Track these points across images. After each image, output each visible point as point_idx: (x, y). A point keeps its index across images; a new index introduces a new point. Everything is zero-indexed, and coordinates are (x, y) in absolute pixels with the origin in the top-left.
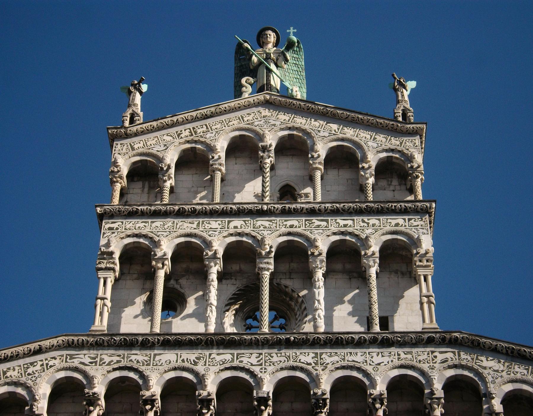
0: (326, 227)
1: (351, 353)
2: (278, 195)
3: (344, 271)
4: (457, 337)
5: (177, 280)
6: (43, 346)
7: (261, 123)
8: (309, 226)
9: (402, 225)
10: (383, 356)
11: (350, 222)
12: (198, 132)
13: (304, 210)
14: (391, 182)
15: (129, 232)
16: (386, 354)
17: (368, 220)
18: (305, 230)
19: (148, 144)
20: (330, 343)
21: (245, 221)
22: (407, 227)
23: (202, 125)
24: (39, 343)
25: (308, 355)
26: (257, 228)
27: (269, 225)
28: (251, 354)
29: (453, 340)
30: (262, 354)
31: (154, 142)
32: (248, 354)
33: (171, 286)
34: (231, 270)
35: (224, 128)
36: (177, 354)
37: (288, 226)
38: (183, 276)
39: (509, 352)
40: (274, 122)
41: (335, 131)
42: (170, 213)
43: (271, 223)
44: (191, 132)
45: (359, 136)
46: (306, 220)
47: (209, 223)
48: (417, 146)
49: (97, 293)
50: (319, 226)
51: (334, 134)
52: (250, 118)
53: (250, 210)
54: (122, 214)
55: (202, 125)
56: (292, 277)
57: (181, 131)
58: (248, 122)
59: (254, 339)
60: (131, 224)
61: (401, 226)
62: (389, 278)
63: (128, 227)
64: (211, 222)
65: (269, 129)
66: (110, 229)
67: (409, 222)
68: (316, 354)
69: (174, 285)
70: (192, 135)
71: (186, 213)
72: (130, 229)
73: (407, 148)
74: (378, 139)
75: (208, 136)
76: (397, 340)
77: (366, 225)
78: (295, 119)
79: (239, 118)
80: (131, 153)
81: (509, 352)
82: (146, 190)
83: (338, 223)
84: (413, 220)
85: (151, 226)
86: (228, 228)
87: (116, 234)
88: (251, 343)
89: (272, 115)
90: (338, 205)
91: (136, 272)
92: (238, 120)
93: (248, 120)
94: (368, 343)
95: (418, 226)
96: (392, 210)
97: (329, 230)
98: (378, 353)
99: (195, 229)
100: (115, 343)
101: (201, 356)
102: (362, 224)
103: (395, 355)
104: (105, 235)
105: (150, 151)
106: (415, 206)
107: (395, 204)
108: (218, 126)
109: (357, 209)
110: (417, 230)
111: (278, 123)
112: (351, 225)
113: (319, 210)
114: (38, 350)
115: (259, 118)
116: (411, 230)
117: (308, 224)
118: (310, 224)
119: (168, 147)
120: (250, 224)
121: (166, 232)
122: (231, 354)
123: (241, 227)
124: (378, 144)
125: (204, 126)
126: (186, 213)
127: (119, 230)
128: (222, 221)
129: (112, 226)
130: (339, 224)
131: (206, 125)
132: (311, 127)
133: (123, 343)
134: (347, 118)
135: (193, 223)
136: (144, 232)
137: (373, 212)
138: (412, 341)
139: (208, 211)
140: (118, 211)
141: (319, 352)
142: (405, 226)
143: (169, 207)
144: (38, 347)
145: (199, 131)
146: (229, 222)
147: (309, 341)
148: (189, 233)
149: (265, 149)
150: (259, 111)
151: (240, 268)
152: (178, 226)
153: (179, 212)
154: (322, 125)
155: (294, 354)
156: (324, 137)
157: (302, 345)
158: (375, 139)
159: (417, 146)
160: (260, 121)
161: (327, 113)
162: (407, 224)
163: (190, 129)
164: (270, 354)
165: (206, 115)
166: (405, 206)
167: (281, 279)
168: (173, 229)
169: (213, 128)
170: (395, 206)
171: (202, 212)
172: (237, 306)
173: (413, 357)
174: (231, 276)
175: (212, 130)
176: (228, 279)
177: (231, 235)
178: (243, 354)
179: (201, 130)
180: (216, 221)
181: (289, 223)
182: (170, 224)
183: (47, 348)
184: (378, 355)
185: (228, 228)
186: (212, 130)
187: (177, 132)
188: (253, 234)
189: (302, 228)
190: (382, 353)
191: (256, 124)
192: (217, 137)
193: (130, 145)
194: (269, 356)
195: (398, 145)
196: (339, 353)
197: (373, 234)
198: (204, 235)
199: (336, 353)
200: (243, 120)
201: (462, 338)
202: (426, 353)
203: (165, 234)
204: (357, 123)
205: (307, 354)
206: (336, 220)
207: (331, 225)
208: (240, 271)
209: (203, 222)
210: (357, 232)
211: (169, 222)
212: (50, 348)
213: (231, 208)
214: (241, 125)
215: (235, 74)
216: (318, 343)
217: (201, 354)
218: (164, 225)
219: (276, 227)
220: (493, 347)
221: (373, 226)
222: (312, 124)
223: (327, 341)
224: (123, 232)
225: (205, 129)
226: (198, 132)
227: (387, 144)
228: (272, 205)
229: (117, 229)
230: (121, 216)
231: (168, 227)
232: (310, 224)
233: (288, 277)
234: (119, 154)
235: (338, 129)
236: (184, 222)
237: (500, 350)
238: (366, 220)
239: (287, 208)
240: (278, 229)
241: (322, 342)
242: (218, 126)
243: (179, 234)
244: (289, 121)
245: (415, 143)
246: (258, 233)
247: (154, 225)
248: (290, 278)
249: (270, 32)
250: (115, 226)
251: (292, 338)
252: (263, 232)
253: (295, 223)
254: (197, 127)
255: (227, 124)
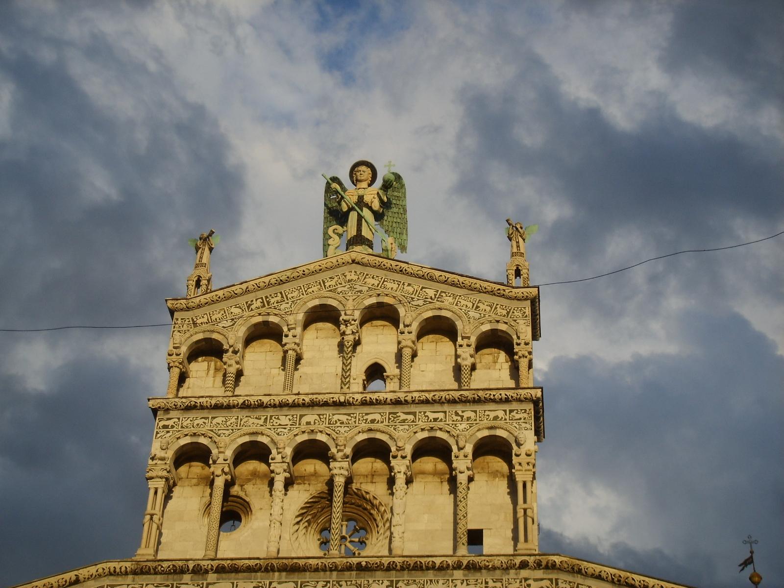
0: (413, 421)
1: (431, 581)
2: (364, 378)
3: (435, 473)
4: (555, 562)
5: (242, 486)
6: (81, 578)
7: (345, 289)
8: (394, 420)
9: (502, 418)
10: (468, 585)
11: (441, 416)
12: (272, 302)
13: (388, 400)
14: (498, 359)
15: (186, 431)
16: (472, 582)
17: (463, 412)
18: (388, 426)
19: (213, 318)
20: (408, 568)
21: (319, 415)
22: (508, 421)
23: (276, 294)
24: (76, 573)
25: (382, 584)
26: (333, 424)
27: (347, 419)
28: (317, 582)
29: (550, 565)
30: (329, 582)
31: (220, 316)
32: (313, 583)
33: (235, 493)
34: (304, 472)
35: (302, 296)
36: (233, 583)
37: (368, 420)
38: (249, 480)
39: (616, 579)
40: (359, 288)
41: (431, 298)
42: (234, 407)
43: (350, 418)
44: (263, 302)
45: (459, 305)
46: (390, 413)
47: (278, 419)
48: (526, 316)
49: (146, 509)
50: (404, 421)
51: (430, 303)
52: (333, 283)
53: (325, 401)
54: (179, 408)
55: (276, 294)
56: (374, 481)
57: (252, 301)
58: (330, 289)
59: (320, 564)
60: (189, 421)
61: (501, 420)
62: (487, 481)
63: (185, 424)
64: (280, 417)
65: (354, 297)
66: (165, 427)
67: (510, 414)
68: (392, 581)
69: (238, 492)
70: (264, 306)
71: (252, 406)
72: (187, 427)
73: (515, 318)
74: (481, 308)
75: (282, 307)
76: (485, 565)
77: (459, 418)
78: (385, 283)
79: (320, 283)
80: (192, 331)
81: (616, 579)
82: (212, 372)
83: (427, 416)
84: (516, 411)
85: (211, 423)
86: (300, 424)
87: (171, 433)
88: (318, 568)
89: (358, 278)
90: (427, 395)
91: (196, 477)
92: (319, 286)
93: (330, 286)
94: (451, 568)
95: (520, 419)
96: (491, 399)
97: (416, 425)
98: (463, 580)
99: (262, 425)
100: (163, 571)
101: (260, 585)
102: (455, 418)
103: (482, 583)
104: (159, 435)
105: (215, 328)
106: (518, 395)
107: (494, 394)
108: (295, 294)
109: (449, 400)
110: (519, 425)
111: (365, 289)
112: (442, 419)
113: (406, 401)
114: (74, 581)
115: (343, 283)
116: (512, 425)
117: (393, 419)
118: (394, 418)
119: (235, 322)
120: (326, 418)
121: (228, 430)
122: (294, 582)
123: (315, 423)
124: (480, 314)
125: (279, 294)
126: (252, 406)
127: (175, 429)
128: (293, 416)
129: (166, 423)
130: (428, 418)
131: (281, 293)
132: (404, 294)
133: (172, 571)
134: (446, 281)
135: (260, 419)
136: (203, 430)
137: (469, 401)
138: (502, 566)
139: (278, 403)
140: (174, 405)
141: (395, 579)
142: (505, 420)
143: (232, 399)
144: (74, 578)
145: (272, 301)
146: (301, 416)
147: (384, 567)
148: (255, 431)
149: (346, 322)
150: (343, 274)
151: (315, 471)
152: (242, 423)
153: (245, 405)
154: (417, 291)
155: (366, 582)
156: (418, 305)
157: (375, 570)
158: (477, 307)
159: (526, 316)
160: (344, 286)
161: (423, 276)
162: (507, 417)
163: (262, 298)
164: (338, 582)
165: (281, 280)
166: (506, 395)
167: (361, 483)
168: (237, 426)
169: (289, 296)
170: (494, 395)
171: (270, 405)
172: (309, 517)
173: (502, 585)
174: (304, 480)
175: (288, 300)
176: (301, 484)
177: (304, 432)
178: (308, 582)
179: (275, 299)
180: (286, 416)
181: (370, 417)
182: (233, 420)
183: (85, 578)
184: (462, 584)
185: (300, 424)
186: (288, 300)
187: (247, 303)
188: (329, 431)
189: (384, 423)
190: (467, 580)
191: (339, 290)
192: (293, 309)
193: (193, 319)
194: (337, 585)
195: (504, 316)
196: (417, 581)
197: (467, 430)
198: (272, 433)
199: (415, 581)
200: (325, 286)
201: (561, 562)
202: (518, 581)
203: (227, 432)
204: (458, 287)
205: (381, 582)
206: (425, 413)
207: (419, 419)
208: (315, 474)
209: (271, 416)
210: (448, 428)
211: (233, 417)
212: (88, 578)
213: (303, 400)
214: (322, 292)
215: (324, 218)
216: (394, 569)
217: (261, 582)
218: (226, 421)
219: (355, 422)
220: (597, 573)
221: (468, 420)
222: (405, 290)
223: (405, 566)
224: (179, 431)
225: (279, 298)
226: (272, 302)
227: (491, 315)
228: (351, 395)
229: (173, 427)
230: (178, 410)
231: (231, 423)
232: (394, 418)
233: (369, 481)
234: (179, 331)
235: (435, 295)
236: (250, 417)
237: (605, 577)
238: (460, 413)
239: (368, 399)
240: (357, 424)
241: (398, 567)
242: (295, 294)
243: (242, 433)
244: (378, 286)
245: (525, 313)
246: (334, 430)
247: (215, 421)
248: (372, 482)
249: (363, 168)
250: (170, 423)
251: (364, 564)
252: (339, 428)
253: (377, 417)
254: (270, 295)
255: (306, 291)
